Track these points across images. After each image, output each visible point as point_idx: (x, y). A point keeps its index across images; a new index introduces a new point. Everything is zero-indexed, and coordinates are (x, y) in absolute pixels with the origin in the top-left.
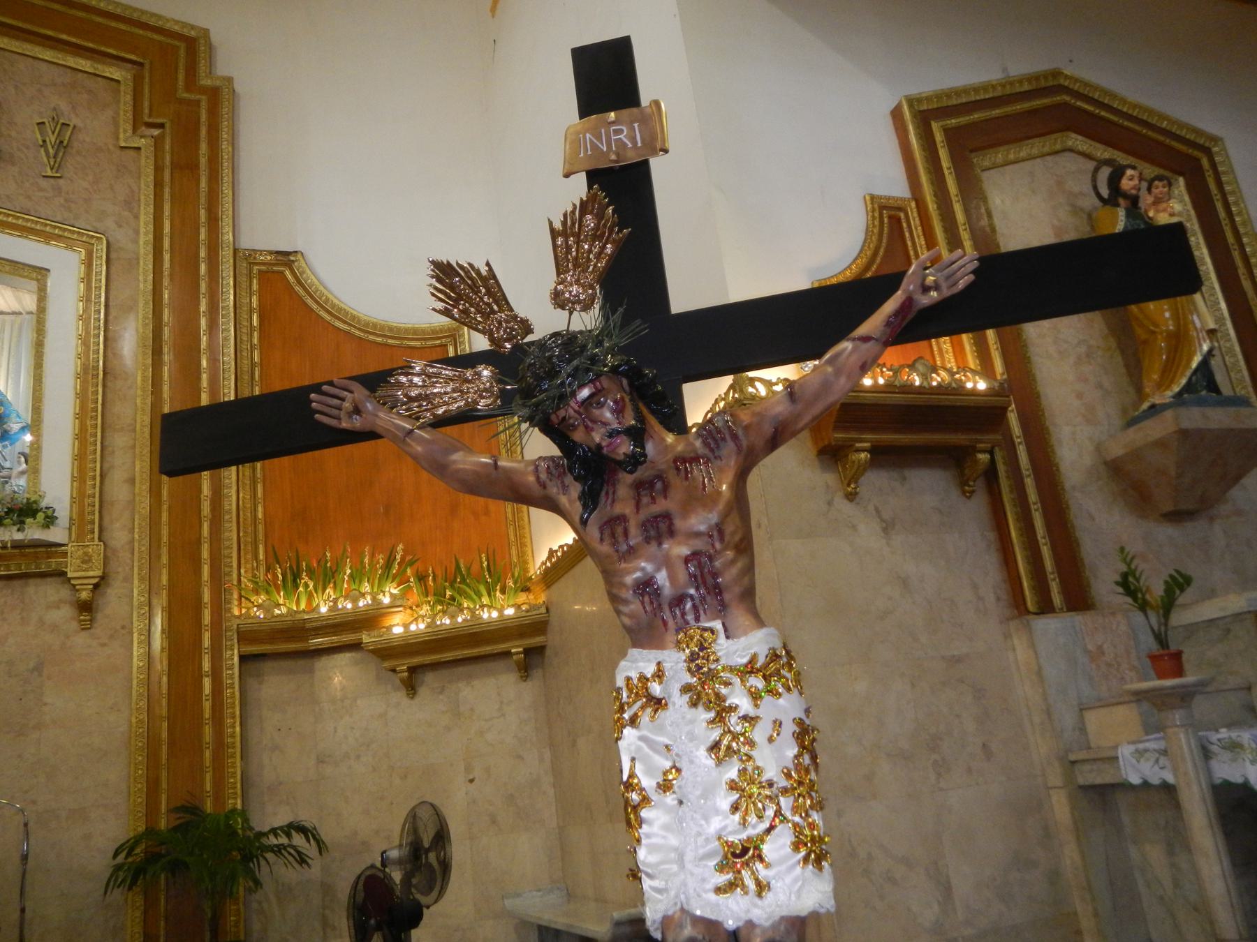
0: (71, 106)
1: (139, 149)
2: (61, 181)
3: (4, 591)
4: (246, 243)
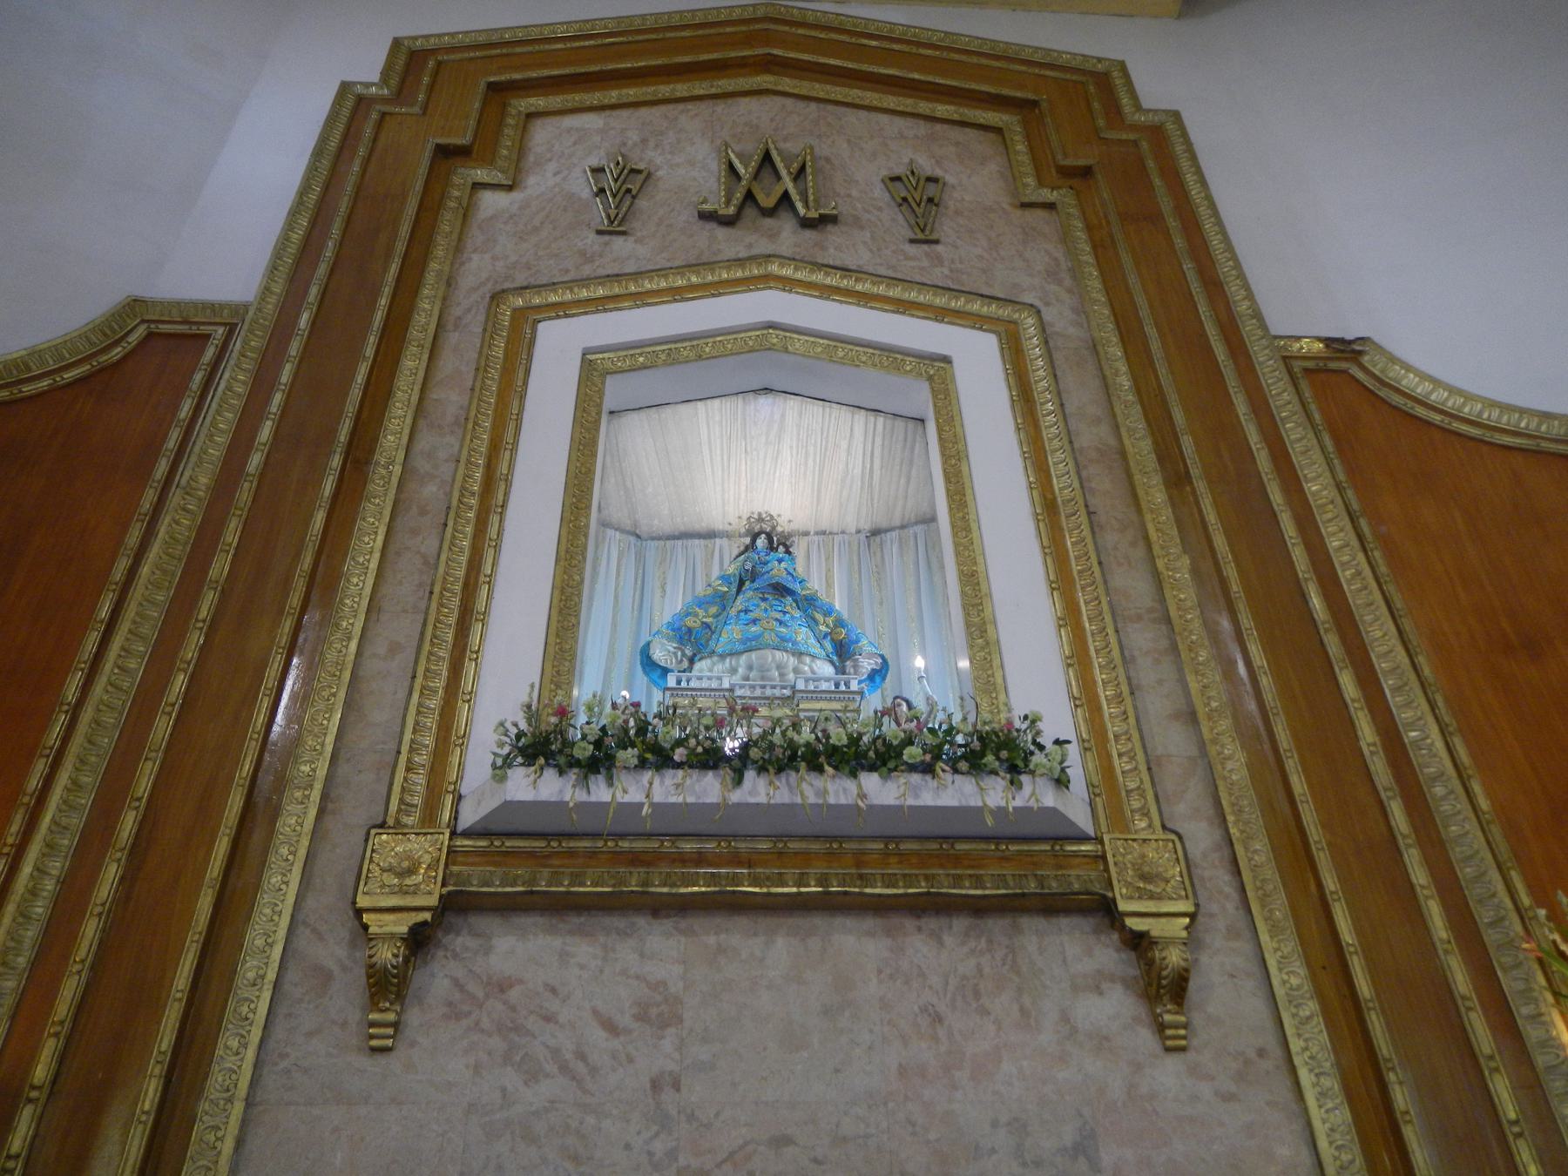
0: (933, 161)
1: (1086, 172)
2: (939, 248)
3: (972, 944)
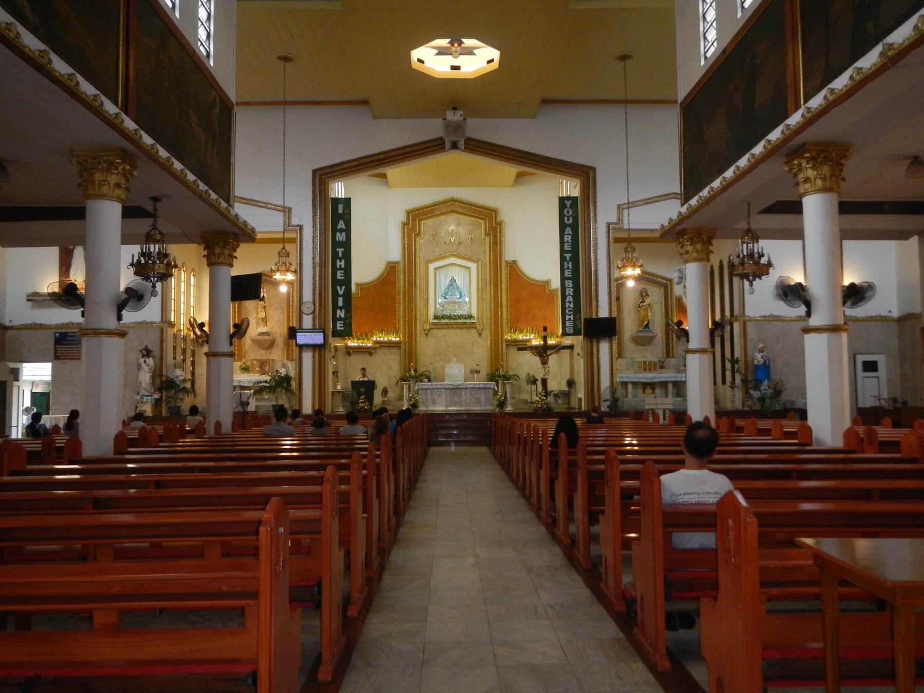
4: (506, 259)
